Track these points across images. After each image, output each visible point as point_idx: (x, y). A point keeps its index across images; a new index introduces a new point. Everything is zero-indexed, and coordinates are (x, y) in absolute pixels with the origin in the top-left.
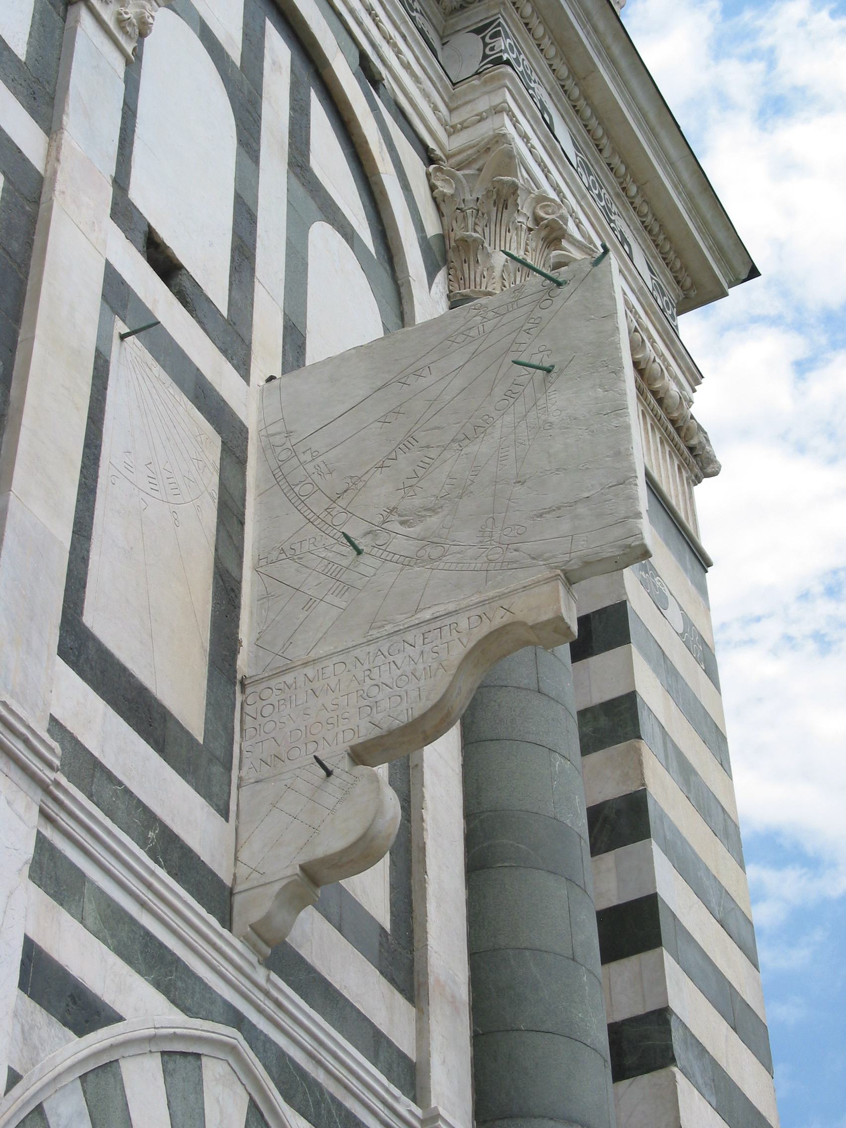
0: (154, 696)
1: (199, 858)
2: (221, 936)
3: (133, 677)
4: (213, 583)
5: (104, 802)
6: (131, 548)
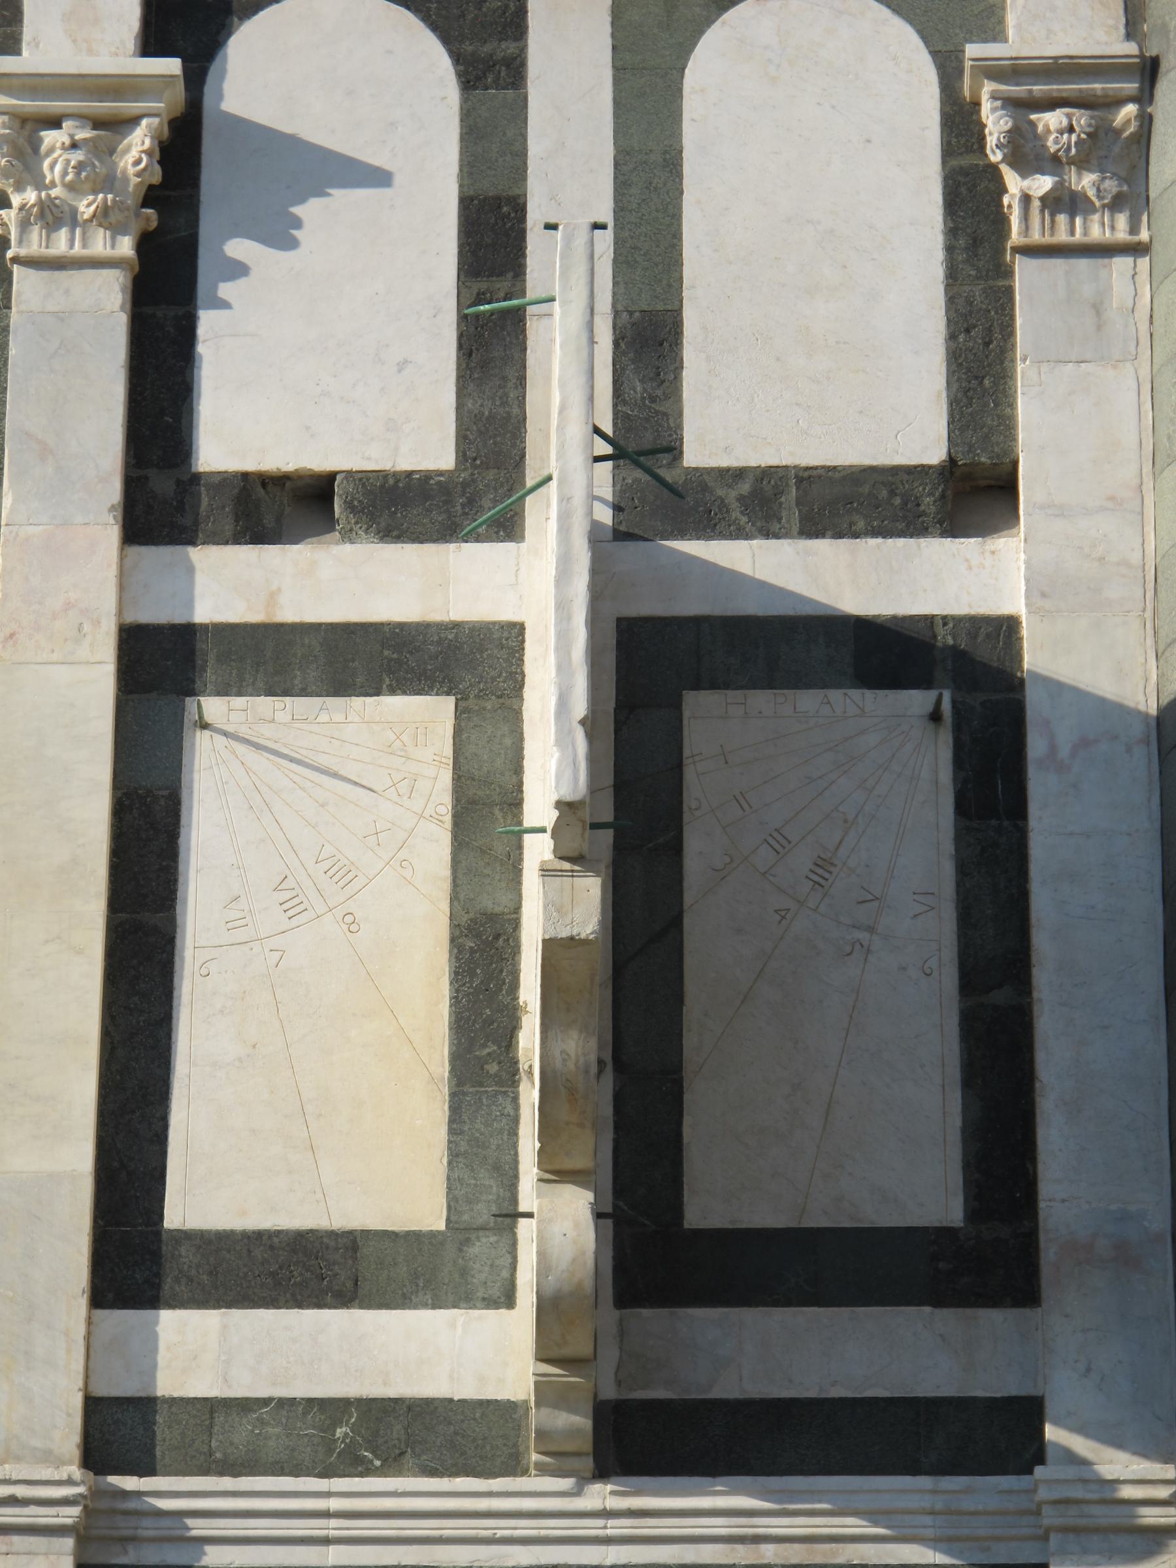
0: (326, 1232)
1: (451, 1400)
2: (490, 1494)
3: (278, 1233)
4: (450, 961)
5: (237, 1448)
6: (254, 1046)
